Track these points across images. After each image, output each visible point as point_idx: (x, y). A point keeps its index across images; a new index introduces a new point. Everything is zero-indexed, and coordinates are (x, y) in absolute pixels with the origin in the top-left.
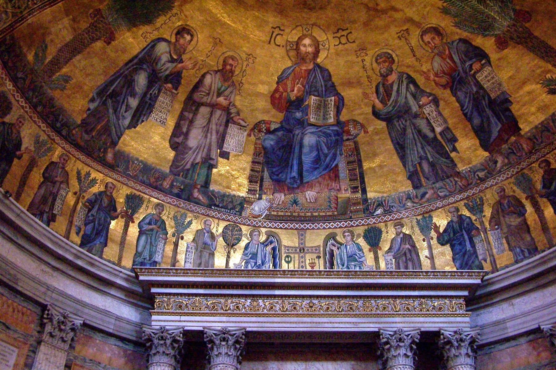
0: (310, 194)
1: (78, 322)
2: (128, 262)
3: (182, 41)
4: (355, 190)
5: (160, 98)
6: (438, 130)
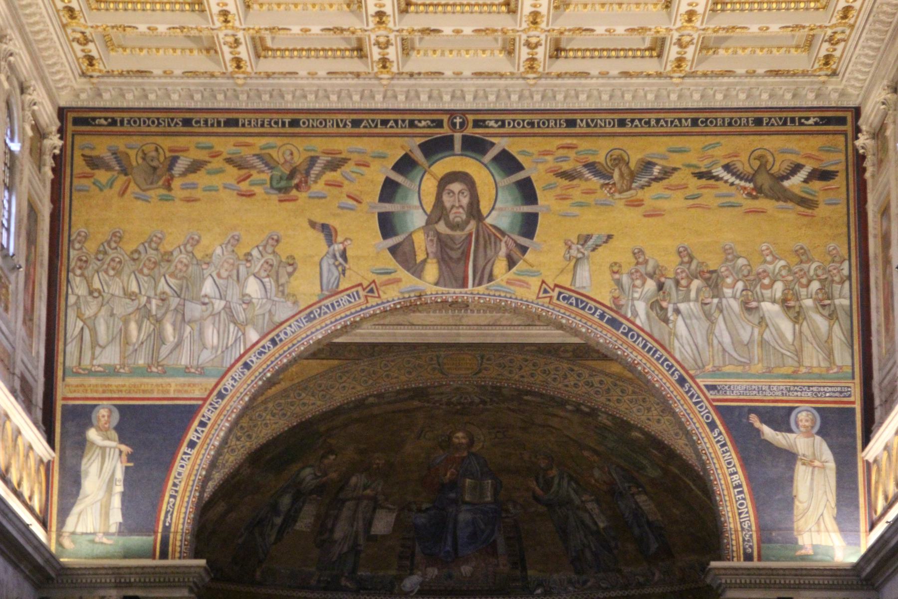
3: (326, 461)
5: (305, 508)
6: (602, 525)
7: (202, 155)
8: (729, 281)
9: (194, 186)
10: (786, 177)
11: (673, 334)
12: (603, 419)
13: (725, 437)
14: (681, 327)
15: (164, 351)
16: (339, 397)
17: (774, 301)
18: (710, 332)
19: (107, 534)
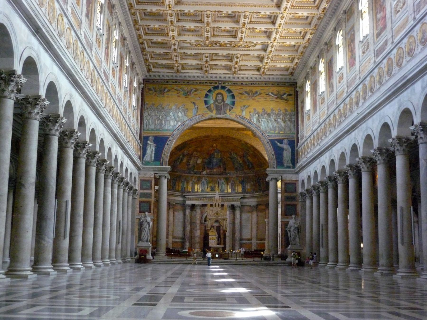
0: (215, 170)
1: (174, 203)
2: (180, 190)
4: (224, 170)
6: (241, 162)
7: (170, 89)
8: (272, 115)
9: (169, 95)
10: (283, 95)
11: (261, 125)
12: (243, 142)
13: (270, 145)
14: (262, 124)
15: (163, 126)
16: (192, 137)
17: (280, 119)
18: (268, 124)
19: (151, 161)
